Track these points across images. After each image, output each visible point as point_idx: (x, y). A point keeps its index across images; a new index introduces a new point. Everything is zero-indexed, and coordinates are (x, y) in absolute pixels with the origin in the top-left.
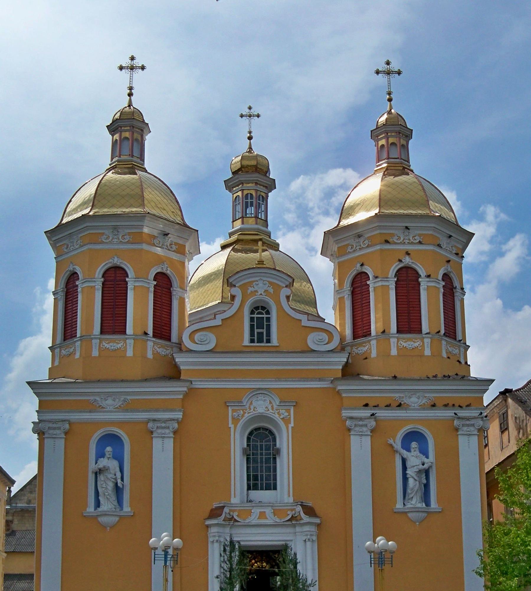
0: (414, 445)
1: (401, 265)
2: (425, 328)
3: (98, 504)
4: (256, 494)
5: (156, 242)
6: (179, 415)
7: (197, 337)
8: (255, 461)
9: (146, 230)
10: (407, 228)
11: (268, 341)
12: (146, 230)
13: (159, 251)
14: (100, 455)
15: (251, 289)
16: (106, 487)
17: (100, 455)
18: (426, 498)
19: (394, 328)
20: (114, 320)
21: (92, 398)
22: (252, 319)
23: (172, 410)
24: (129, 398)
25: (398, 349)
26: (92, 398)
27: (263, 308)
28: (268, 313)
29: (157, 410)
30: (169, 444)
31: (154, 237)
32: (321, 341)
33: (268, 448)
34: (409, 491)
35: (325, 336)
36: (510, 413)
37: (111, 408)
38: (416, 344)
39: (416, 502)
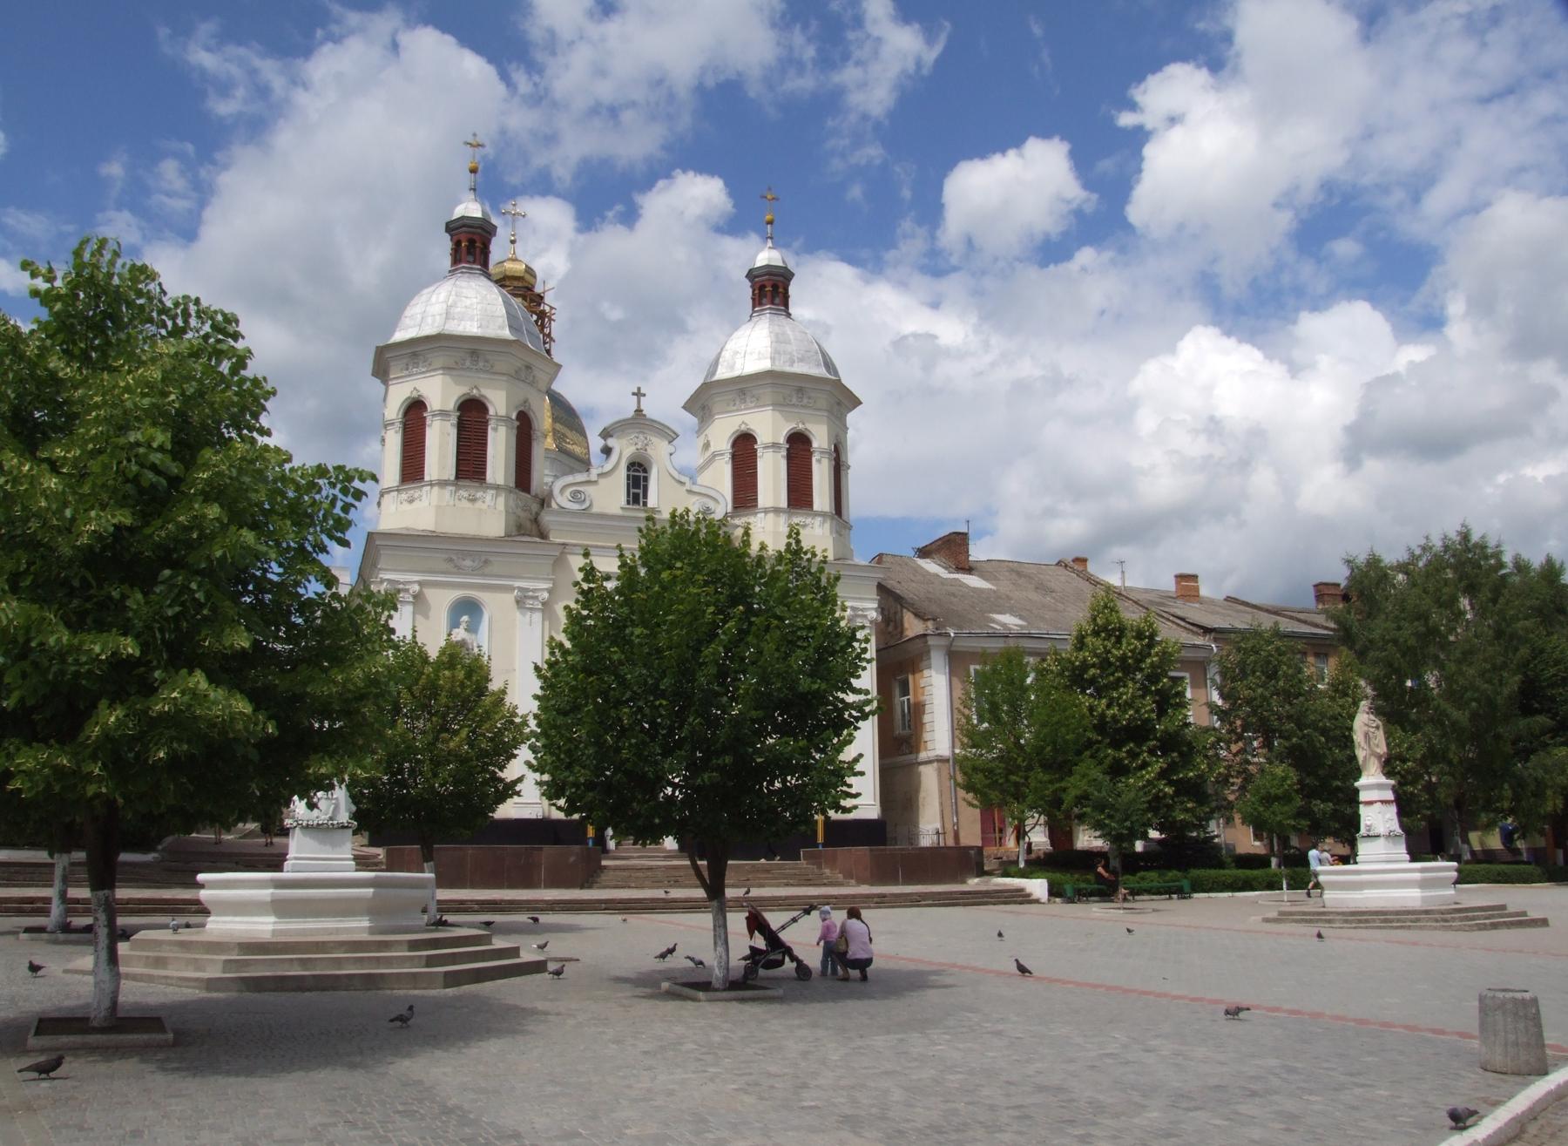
2: (816, 507)
11: (645, 504)
17: (454, 624)
20: (470, 465)
27: (640, 465)
28: (645, 471)
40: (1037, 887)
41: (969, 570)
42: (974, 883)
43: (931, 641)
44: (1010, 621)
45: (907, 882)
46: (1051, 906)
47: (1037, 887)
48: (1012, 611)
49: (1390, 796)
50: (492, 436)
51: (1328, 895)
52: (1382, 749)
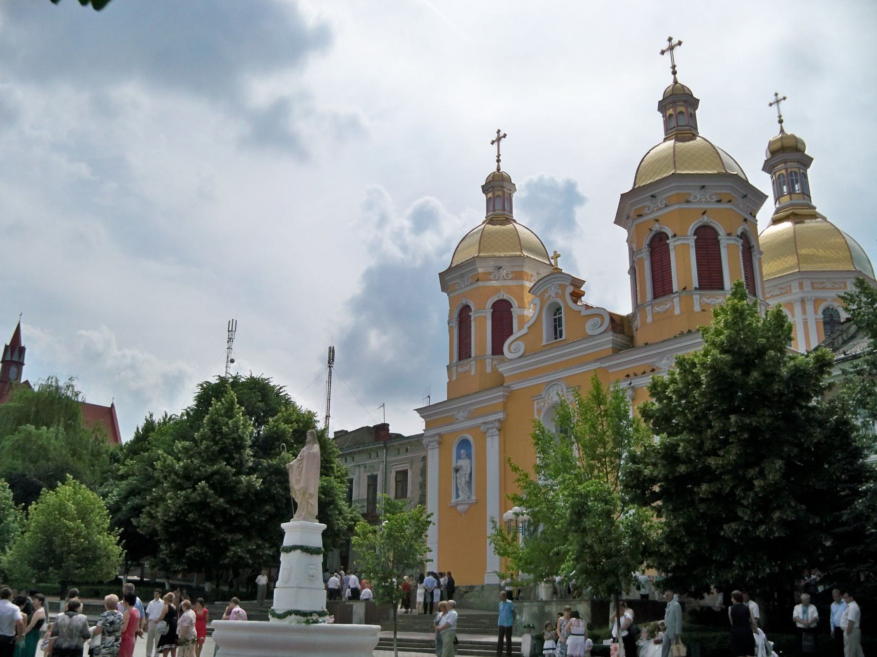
1: (653, 233)
3: (458, 496)
5: (491, 277)
6: (501, 416)
9: (480, 270)
10: (652, 196)
12: (480, 270)
13: (494, 283)
14: (459, 457)
15: (547, 295)
16: (463, 481)
17: (459, 457)
21: (451, 414)
23: (496, 413)
24: (472, 408)
25: (653, 316)
26: (451, 414)
29: (487, 415)
30: (496, 440)
31: (490, 273)
32: (594, 325)
35: (598, 319)
37: (462, 419)
38: (668, 306)
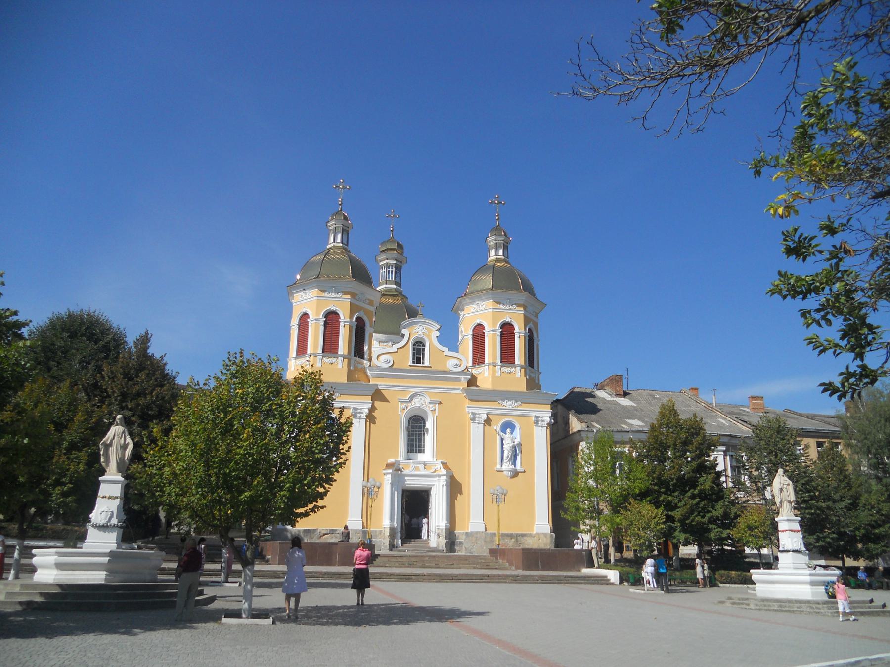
0: (508, 430)
4: (412, 455)
7: (382, 358)
8: (412, 435)
18: (514, 464)
19: (498, 360)
22: (414, 349)
27: (421, 343)
28: (424, 346)
33: (420, 427)
34: (505, 458)
35: (457, 361)
36: (559, 414)
39: (507, 466)
40: (613, 575)
41: (625, 394)
42: (586, 571)
43: (584, 435)
44: (636, 423)
45: (543, 569)
46: (622, 587)
47: (613, 575)
48: (640, 419)
49: (797, 526)
50: (341, 330)
51: (758, 587)
52: (792, 497)
